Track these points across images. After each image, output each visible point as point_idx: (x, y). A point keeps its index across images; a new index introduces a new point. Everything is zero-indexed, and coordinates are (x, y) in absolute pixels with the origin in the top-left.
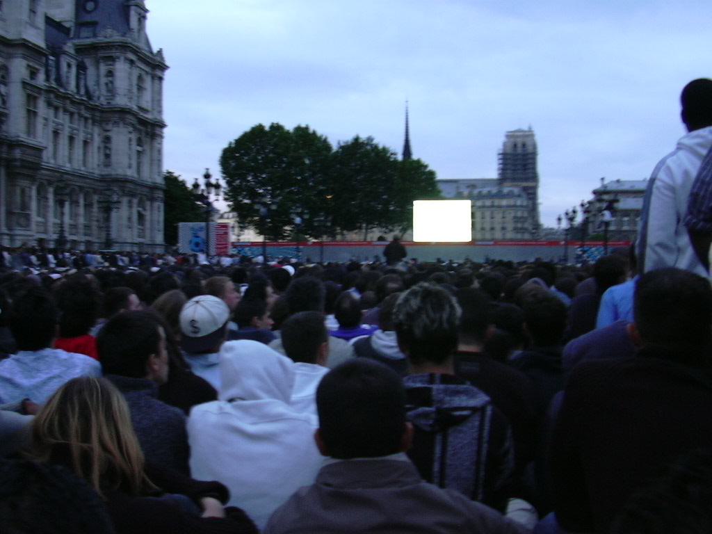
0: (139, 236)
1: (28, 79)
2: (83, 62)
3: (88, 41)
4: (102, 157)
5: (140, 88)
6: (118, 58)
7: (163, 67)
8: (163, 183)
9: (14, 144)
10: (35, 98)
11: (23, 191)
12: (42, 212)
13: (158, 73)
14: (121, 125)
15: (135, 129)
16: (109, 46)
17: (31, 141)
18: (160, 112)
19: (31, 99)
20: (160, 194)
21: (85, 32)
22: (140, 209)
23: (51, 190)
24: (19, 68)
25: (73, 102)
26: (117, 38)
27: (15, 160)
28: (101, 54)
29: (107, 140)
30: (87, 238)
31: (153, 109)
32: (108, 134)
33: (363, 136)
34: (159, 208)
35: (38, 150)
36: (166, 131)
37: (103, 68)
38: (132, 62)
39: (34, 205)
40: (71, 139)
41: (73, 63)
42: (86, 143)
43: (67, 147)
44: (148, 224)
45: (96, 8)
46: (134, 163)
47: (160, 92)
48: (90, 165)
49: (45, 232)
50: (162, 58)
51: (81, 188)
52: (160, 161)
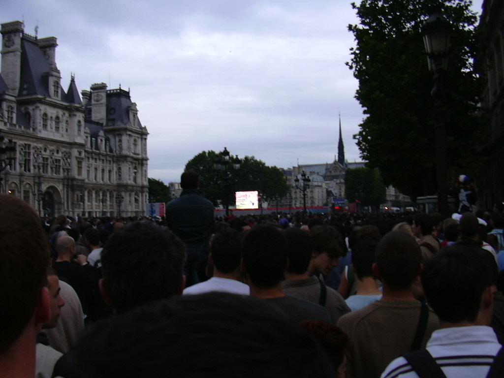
0: (136, 208)
1: (79, 156)
2: (108, 138)
3: (112, 127)
4: (118, 175)
5: (135, 145)
6: (123, 134)
7: (147, 134)
8: (148, 184)
9: (73, 179)
10: (81, 162)
11: (77, 195)
12: (90, 200)
13: (144, 137)
14: (125, 162)
15: (132, 163)
16: (120, 129)
17: (80, 178)
18: (146, 153)
19: (80, 163)
20: (147, 190)
21: (110, 124)
22: (136, 197)
23: (94, 192)
24: (75, 152)
25: (103, 155)
26: (123, 126)
27: (74, 185)
28: (116, 133)
29: (119, 169)
30: (112, 210)
31: (142, 153)
32: (120, 166)
33: (250, 156)
34: (146, 196)
35: (83, 180)
36: (149, 162)
38: (130, 135)
39: (86, 198)
40: (103, 170)
41: (103, 139)
42: (110, 171)
43: (101, 173)
44: (140, 203)
45: (115, 112)
46: (132, 178)
47: (145, 145)
48: (112, 180)
49: (92, 208)
50: (146, 130)
51: (108, 190)
52: (146, 175)
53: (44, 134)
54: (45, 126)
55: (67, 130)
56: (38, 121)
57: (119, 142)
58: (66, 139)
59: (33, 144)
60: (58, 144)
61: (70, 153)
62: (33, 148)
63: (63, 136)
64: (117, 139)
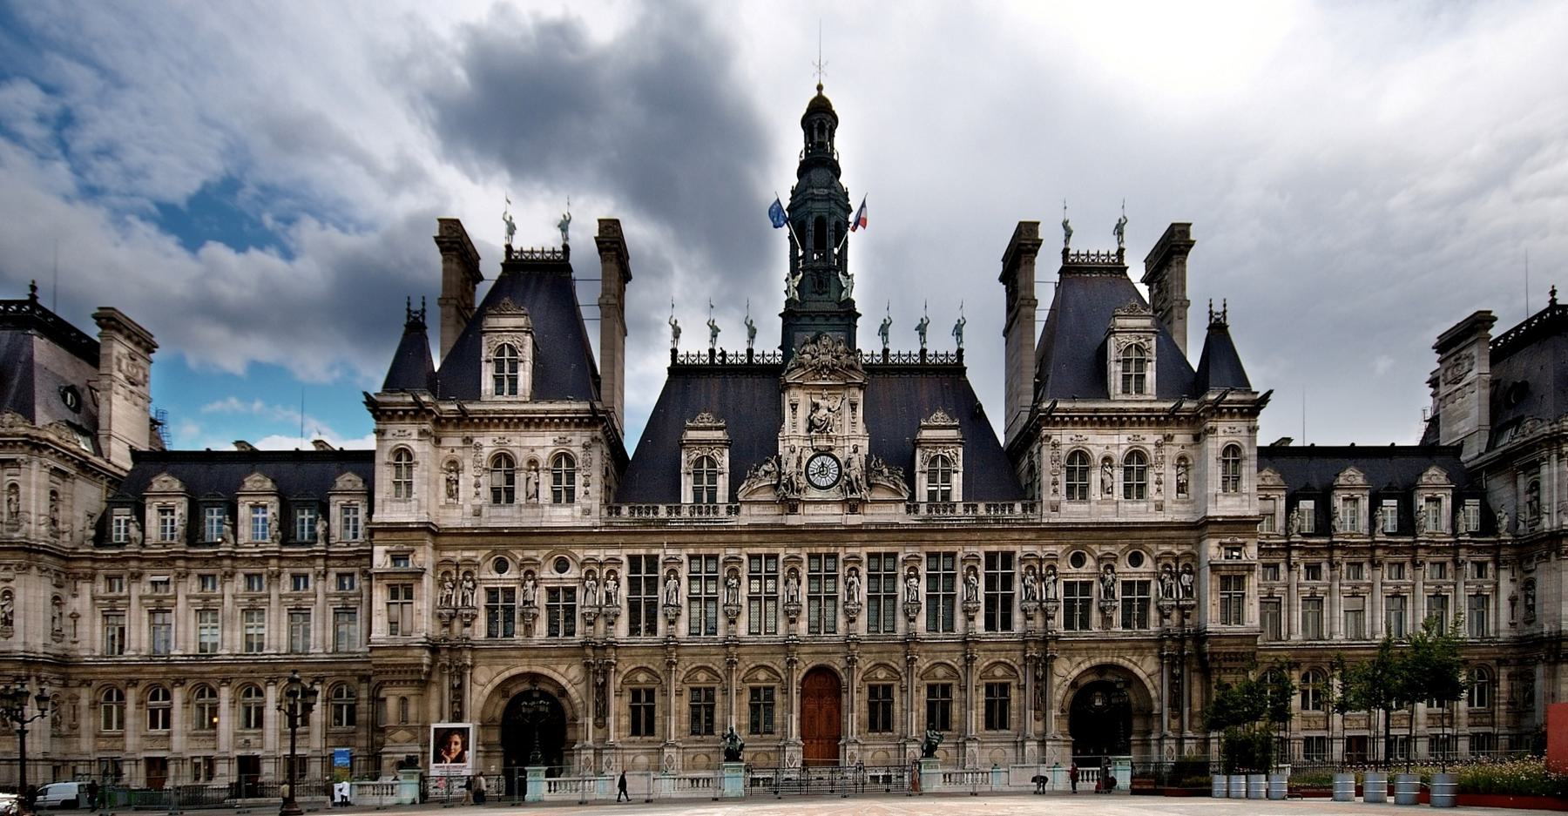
37: (1523, 483)
53: (1074, 512)
54: (1078, 491)
55: (1181, 488)
56: (1046, 478)
57: (1530, 491)
58: (1176, 512)
59: (1020, 551)
60: (1137, 534)
61: (1195, 558)
62: (1022, 560)
63: (1160, 507)
64: (1523, 483)
